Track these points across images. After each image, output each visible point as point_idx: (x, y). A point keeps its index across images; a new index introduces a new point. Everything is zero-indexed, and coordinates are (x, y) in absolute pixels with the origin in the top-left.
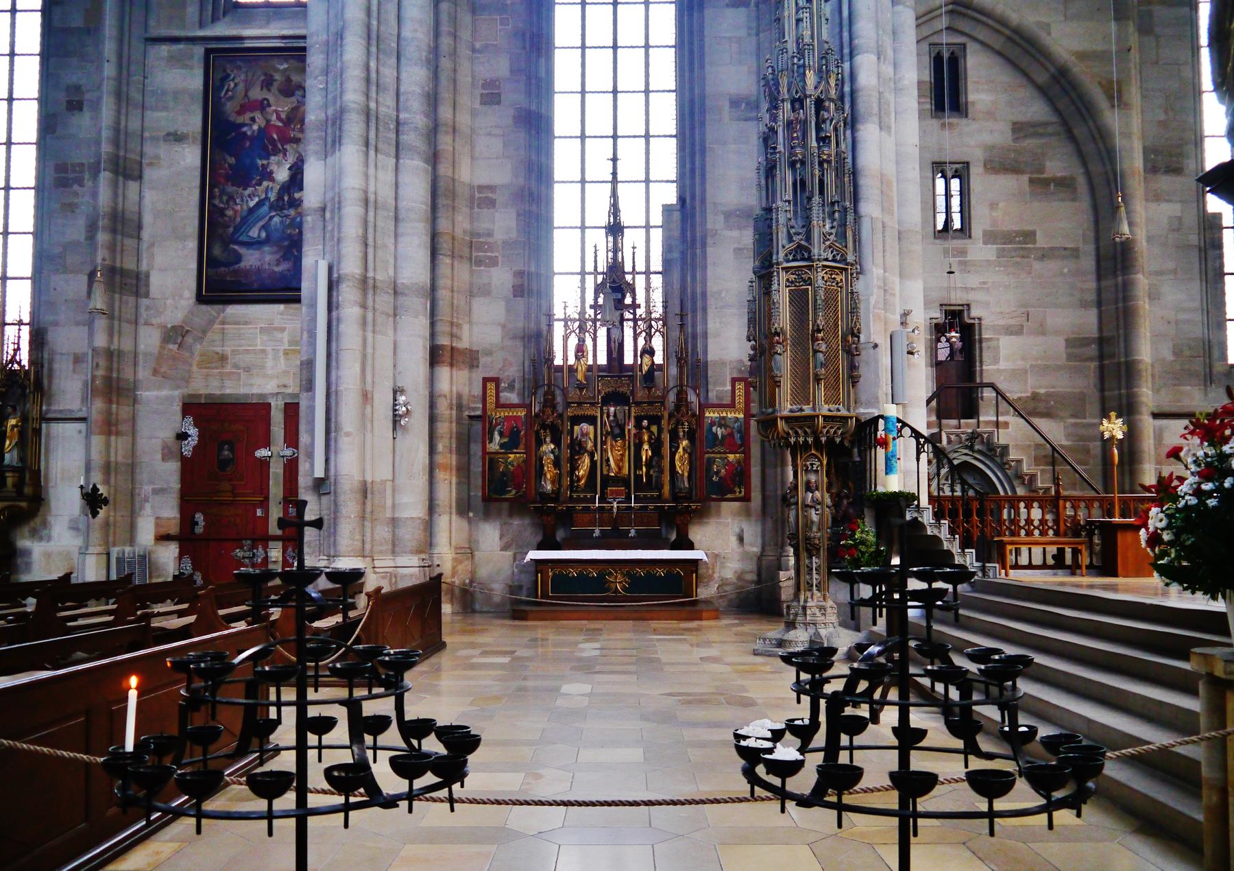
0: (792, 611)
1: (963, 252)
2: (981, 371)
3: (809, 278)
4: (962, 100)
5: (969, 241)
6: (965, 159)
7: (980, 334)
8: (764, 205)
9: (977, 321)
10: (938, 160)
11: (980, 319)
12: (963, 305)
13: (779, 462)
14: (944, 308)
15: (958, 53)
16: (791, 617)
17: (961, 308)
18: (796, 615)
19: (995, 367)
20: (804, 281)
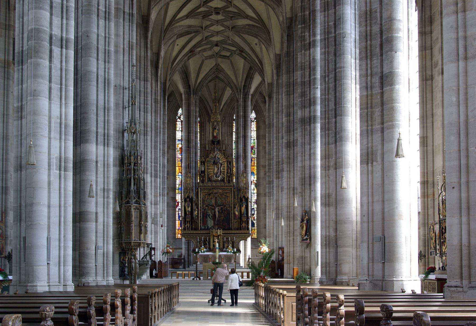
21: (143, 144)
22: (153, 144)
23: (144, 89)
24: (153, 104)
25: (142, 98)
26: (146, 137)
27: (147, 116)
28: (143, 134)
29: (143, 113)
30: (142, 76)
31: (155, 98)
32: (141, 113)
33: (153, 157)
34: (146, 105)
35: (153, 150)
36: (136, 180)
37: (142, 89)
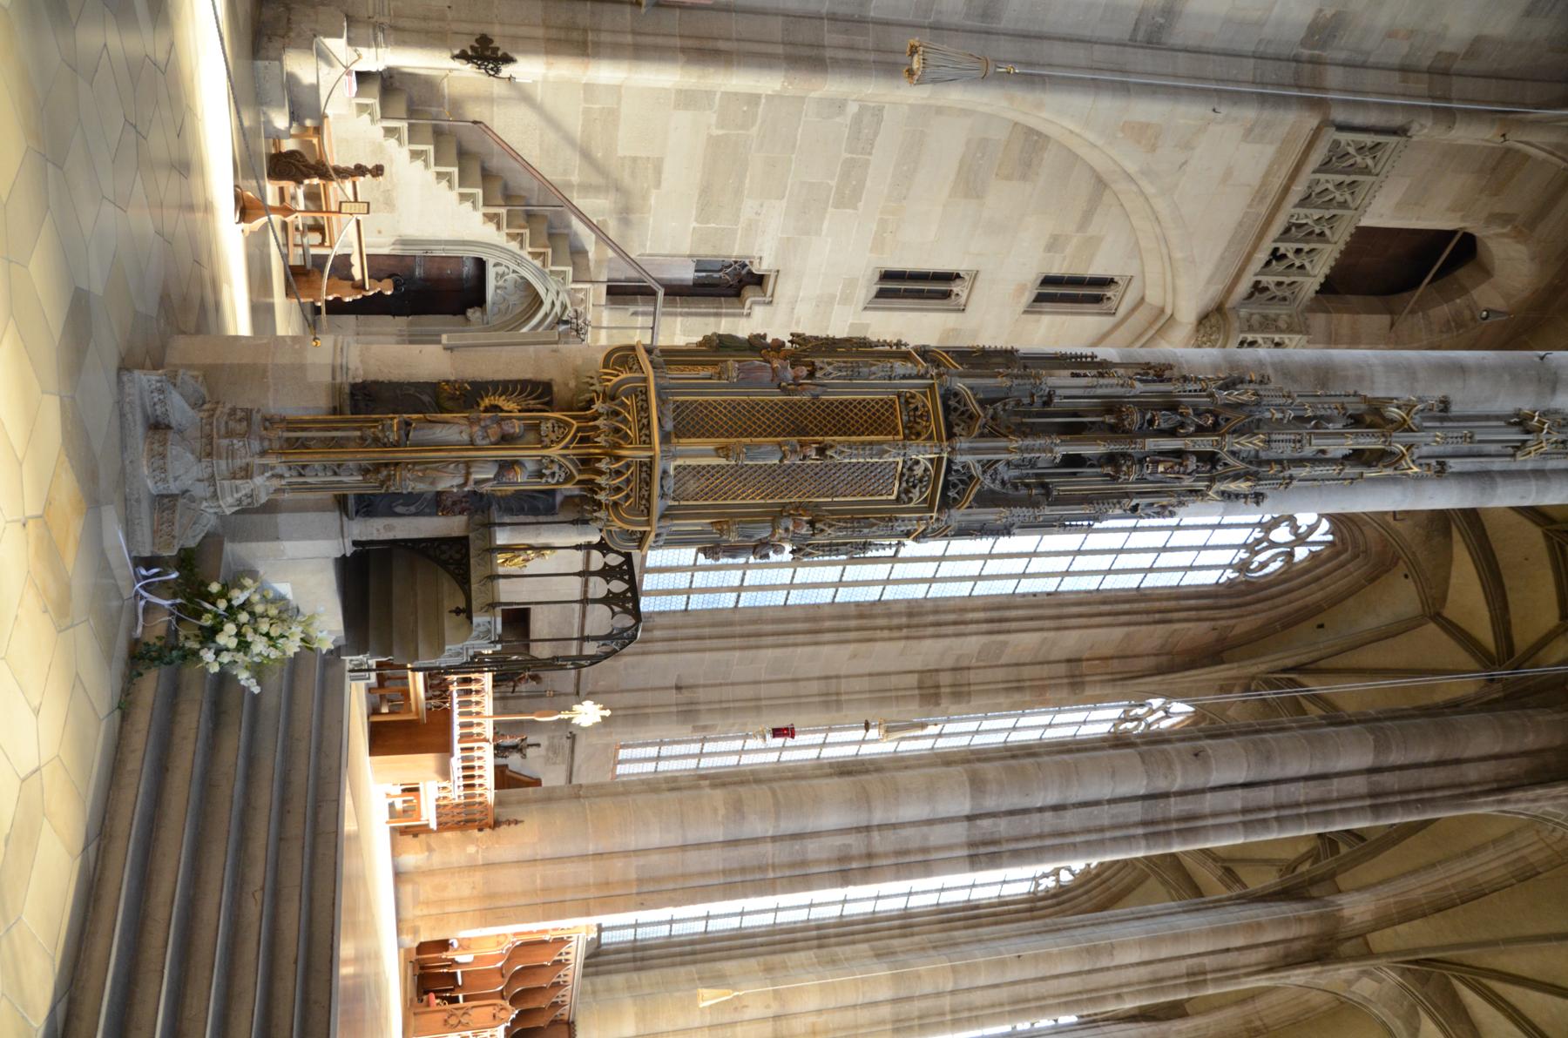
0: (237, 443)
1: (846, 300)
2: (675, 314)
3: (911, 500)
4: (1047, 306)
5: (861, 306)
6: (969, 309)
7: (727, 315)
8: (1059, 392)
9: (746, 311)
10: (980, 277)
11: (749, 315)
12: (772, 296)
13: (553, 33)
14: (773, 275)
15: (1105, 306)
16: (225, 442)
17: (769, 292)
18: (232, 454)
19: (678, 331)
20: (907, 491)
21: (1106, 822)
22: (1031, 990)
23: (1339, 800)
24: (1182, 967)
25: (1300, 792)
26: (1140, 831)
27: (1231, 826)
28: (1149, 817)
29: (1238, 805)
30: (1389, 780)
31: (1205, 973)
32: (1239, 792)
33: (977, 998)
34: (1278, 819)
35: (1004, 994)
36: (1110, 419)
37: (1336, 787)
